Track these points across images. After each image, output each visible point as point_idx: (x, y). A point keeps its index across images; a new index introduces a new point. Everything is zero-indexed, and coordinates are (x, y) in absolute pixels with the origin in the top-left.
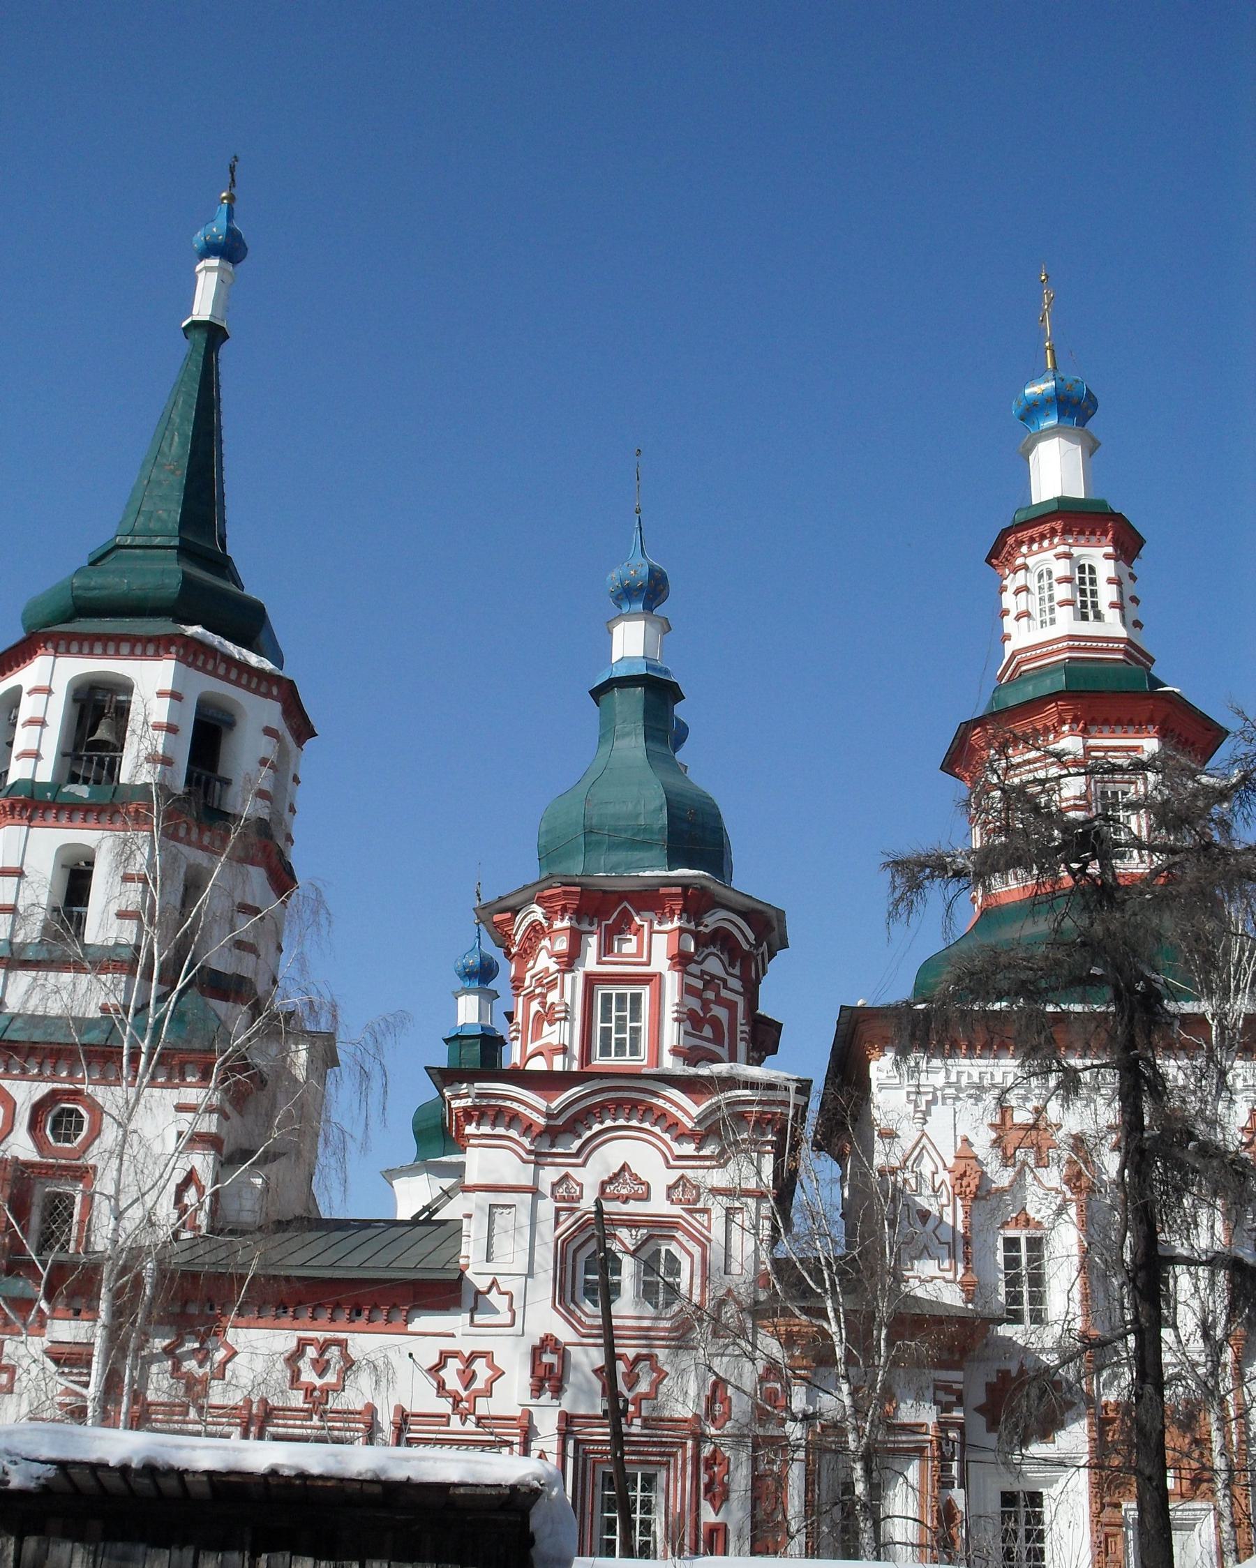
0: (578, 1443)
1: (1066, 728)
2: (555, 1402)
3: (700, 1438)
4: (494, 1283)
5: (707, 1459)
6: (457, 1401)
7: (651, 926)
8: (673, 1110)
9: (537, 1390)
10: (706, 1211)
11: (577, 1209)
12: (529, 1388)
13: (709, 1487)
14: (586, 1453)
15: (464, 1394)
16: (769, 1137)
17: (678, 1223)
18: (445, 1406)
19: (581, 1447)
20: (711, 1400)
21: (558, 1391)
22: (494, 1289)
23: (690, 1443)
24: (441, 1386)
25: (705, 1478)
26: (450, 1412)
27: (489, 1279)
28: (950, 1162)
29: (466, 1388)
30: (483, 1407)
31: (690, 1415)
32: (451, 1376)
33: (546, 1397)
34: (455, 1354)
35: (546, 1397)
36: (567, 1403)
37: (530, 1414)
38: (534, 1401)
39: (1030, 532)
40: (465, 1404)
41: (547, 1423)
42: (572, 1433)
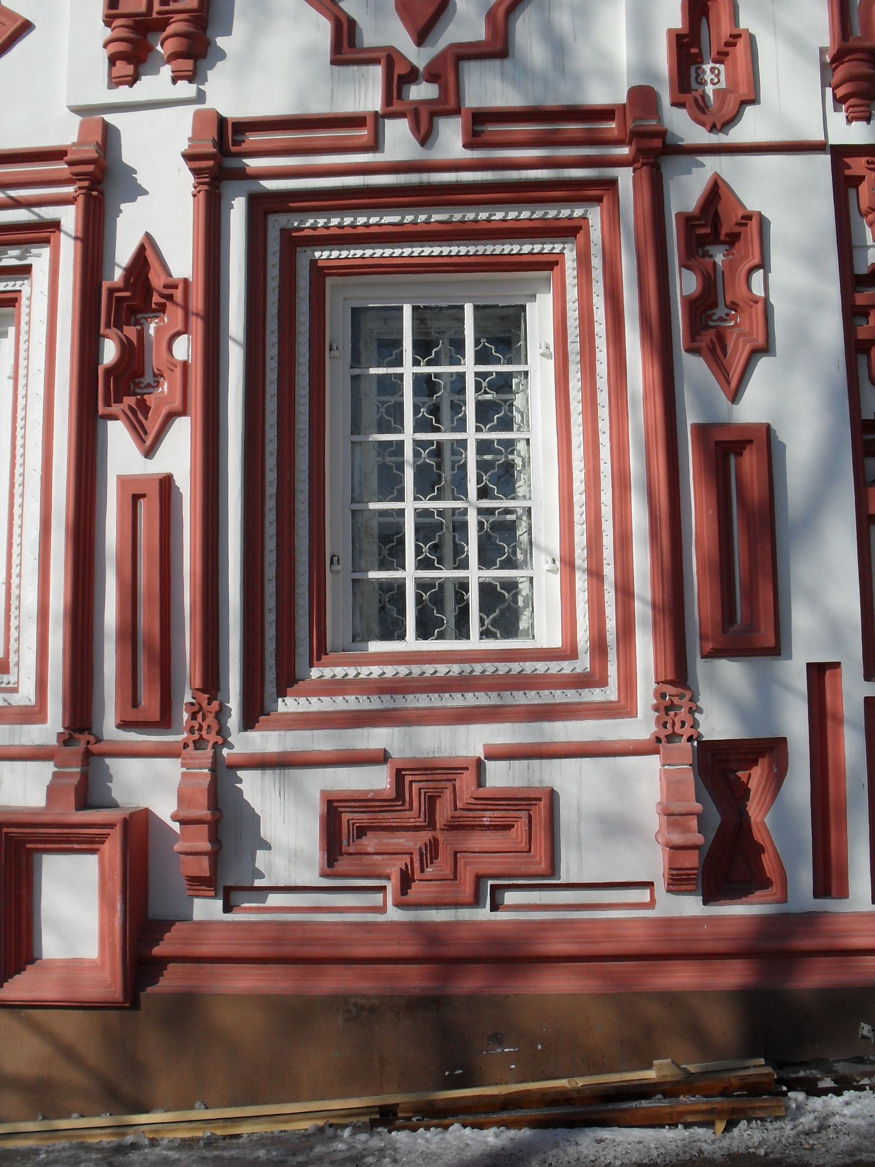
0: (262, 207)
3: (656, 153)
5: (688, 221)
9: (131, 54)
12: (103, 56)
13: (702, 308)
14: (293, 243)
19: (277, 223)
20: (687, 49)
21: (197, 54)
23: (625, 177)
25: (685, 284)
31: (622, 98)
35: (158, 83)
36: (230, 92)
37: (109, 137)
41: (158, 144)
42: (242, 175)
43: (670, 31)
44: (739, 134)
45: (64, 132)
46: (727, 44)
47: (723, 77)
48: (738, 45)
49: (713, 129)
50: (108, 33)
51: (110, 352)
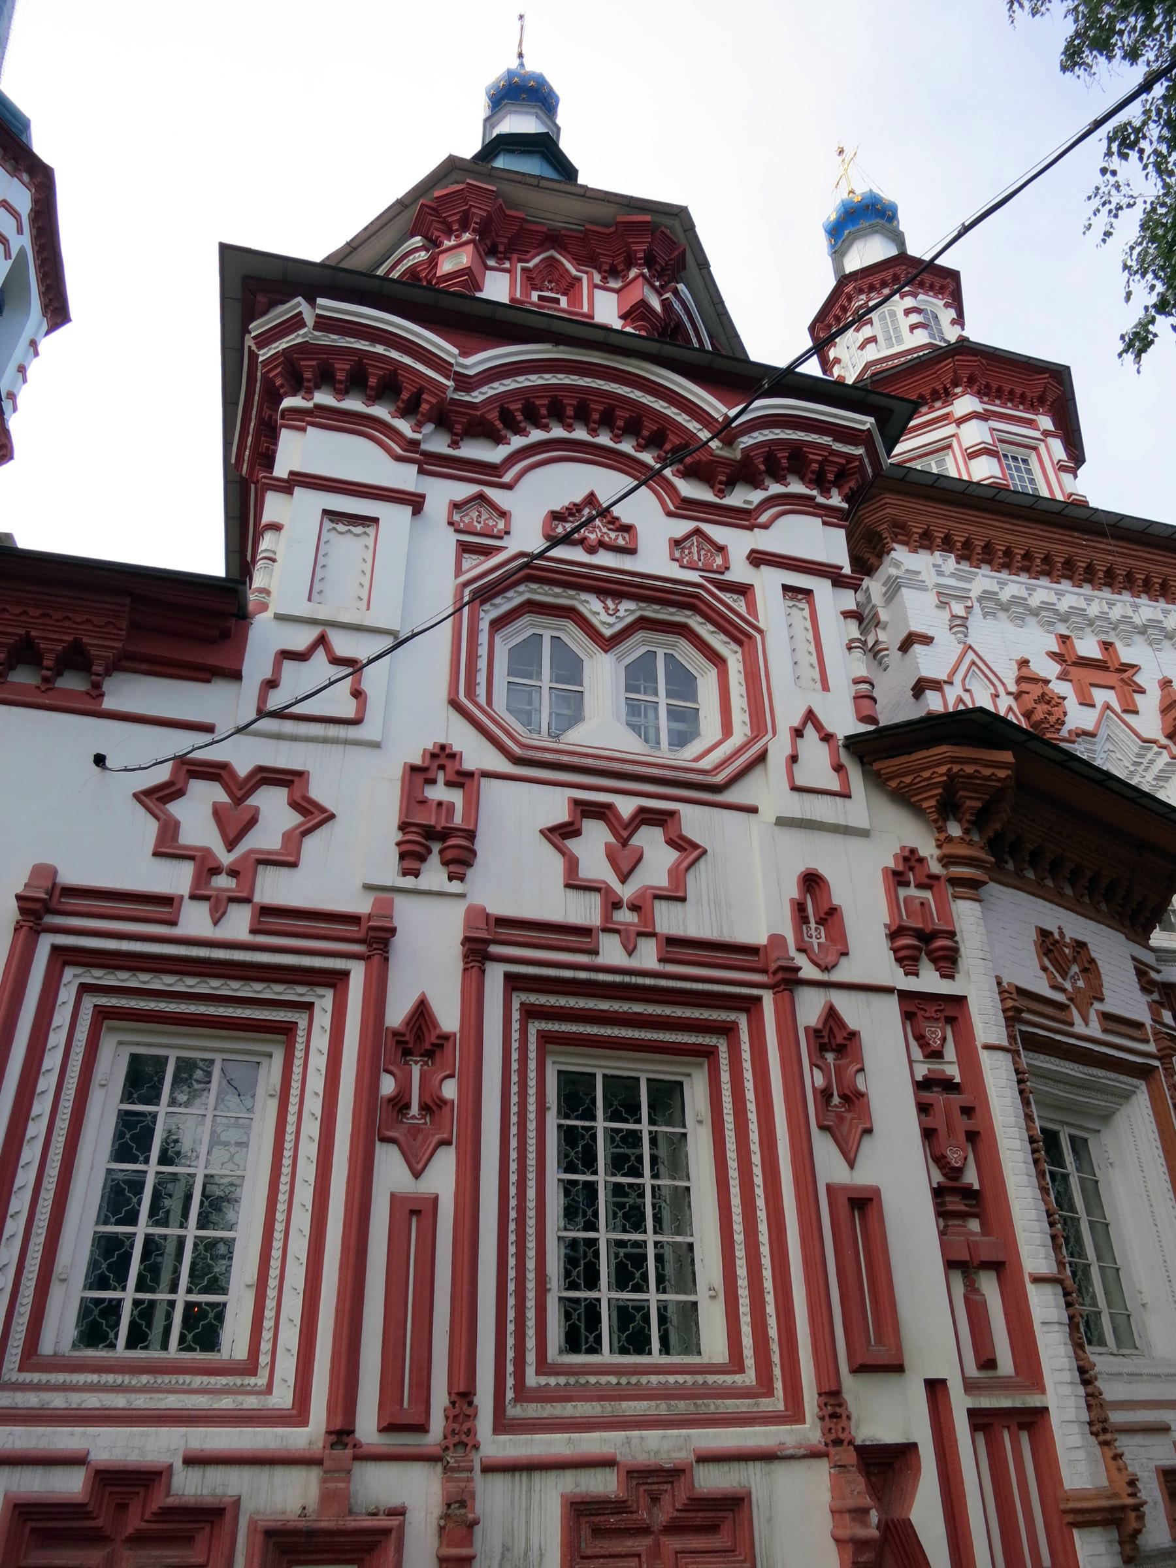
1: (958, 390)
2: (456, 887)
4: (322, 640)
5: (814, 1033)
6: (207, 868)
7: (591, 279)
8: (682, 418)
10: (744, 590)
11: (500, 549)
15: (226, 859)
16: (836, 500)
17: (697, 596)
18: (176, 879)
22: (320, 653)
24: (169, 829)
26: (186, 892)
27: (312, 634)
28: (1013, 688)
29: (231, 845)
30: (275, 888)
32: (196, 813)
33: (434, 875)
34: (216, 772)
38: (408, 882)
39: (871, 279)
40: (223, 882)
43: (792, 900)
44: (837, 976)
45: (362, 905)
46: (826, 913)
47: (823, 934)
48: (830, 916)
49: (826, 969)
50: (399, 836)
51: (388, 1086)
